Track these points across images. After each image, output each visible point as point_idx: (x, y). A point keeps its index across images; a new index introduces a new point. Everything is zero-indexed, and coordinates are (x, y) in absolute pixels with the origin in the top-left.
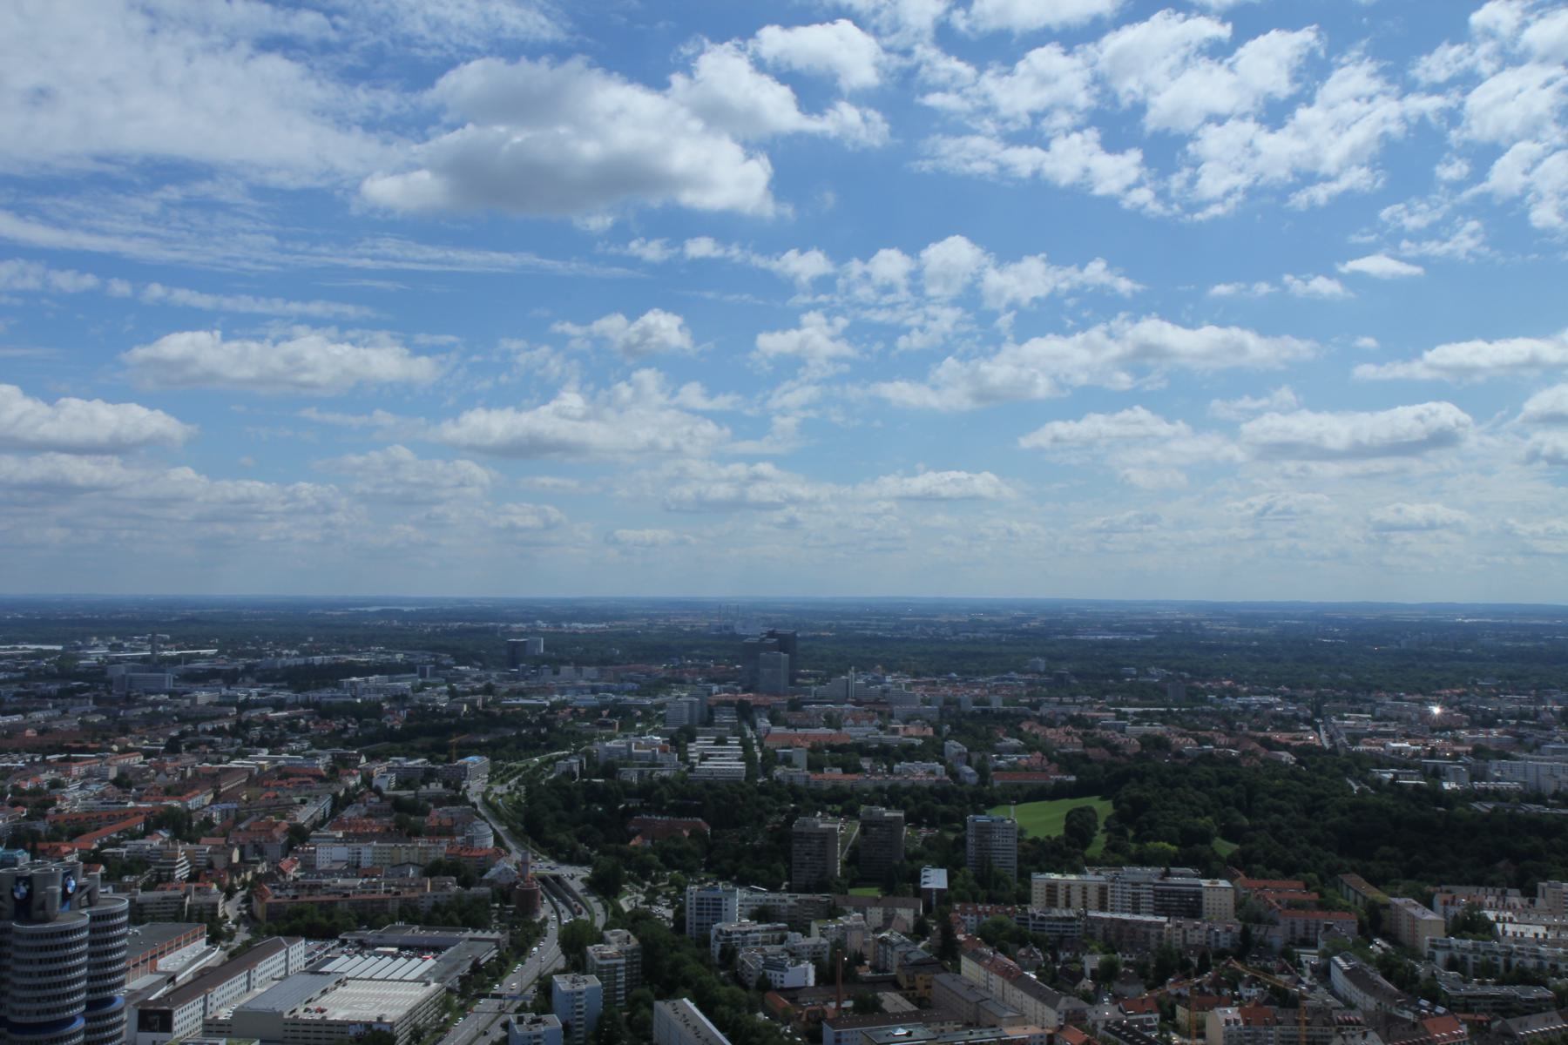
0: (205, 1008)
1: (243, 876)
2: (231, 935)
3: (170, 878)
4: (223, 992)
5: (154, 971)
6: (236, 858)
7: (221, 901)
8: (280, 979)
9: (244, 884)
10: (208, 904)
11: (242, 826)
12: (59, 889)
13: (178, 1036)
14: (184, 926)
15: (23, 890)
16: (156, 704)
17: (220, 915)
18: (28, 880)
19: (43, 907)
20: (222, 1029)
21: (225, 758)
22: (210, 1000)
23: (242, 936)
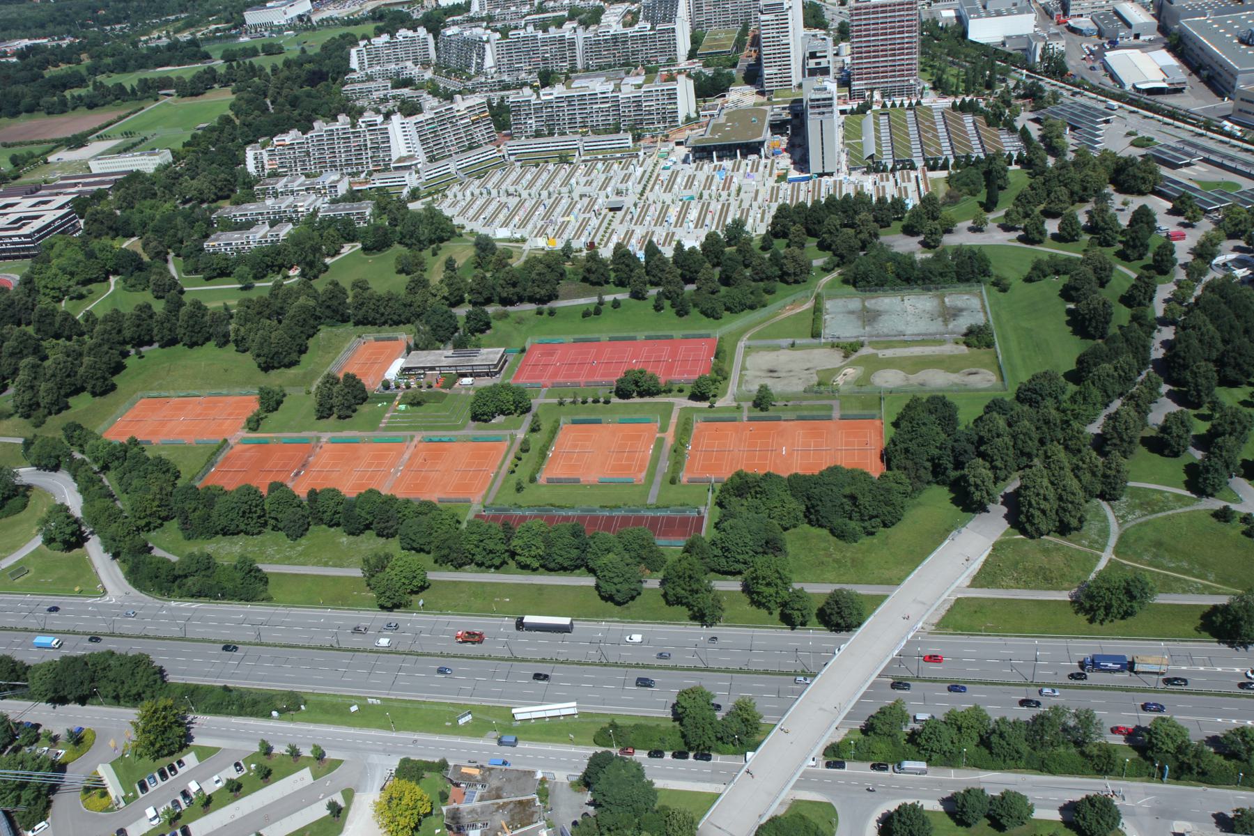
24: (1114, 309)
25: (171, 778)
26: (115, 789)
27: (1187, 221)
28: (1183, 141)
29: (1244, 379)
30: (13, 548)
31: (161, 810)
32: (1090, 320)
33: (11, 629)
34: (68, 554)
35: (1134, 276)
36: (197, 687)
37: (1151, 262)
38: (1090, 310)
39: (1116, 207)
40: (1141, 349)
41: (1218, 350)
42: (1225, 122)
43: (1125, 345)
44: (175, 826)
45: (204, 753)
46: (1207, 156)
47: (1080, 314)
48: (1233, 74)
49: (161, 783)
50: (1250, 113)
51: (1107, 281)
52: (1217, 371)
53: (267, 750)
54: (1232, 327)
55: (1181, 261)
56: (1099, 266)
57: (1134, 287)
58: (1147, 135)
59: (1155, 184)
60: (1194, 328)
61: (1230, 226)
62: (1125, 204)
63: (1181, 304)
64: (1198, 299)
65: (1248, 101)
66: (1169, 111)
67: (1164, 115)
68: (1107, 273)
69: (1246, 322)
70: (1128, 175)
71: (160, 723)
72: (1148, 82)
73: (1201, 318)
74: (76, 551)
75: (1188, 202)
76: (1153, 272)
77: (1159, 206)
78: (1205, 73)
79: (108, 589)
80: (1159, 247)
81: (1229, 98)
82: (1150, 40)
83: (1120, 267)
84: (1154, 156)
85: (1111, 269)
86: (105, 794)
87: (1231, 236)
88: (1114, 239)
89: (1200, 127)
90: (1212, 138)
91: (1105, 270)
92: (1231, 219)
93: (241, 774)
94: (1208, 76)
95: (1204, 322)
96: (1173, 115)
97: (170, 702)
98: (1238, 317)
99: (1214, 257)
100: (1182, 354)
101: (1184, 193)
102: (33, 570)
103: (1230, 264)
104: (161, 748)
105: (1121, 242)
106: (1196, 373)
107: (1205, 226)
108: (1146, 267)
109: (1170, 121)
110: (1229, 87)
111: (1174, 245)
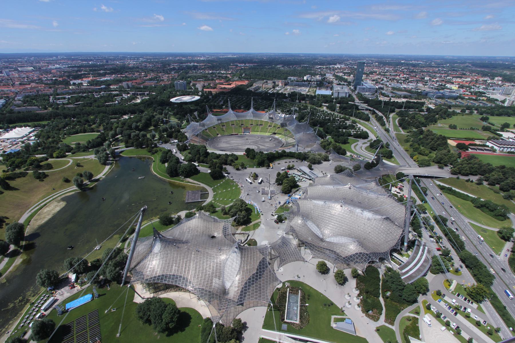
25: (466, 302)
26: (452, 287)
30: (489, 226)
31: (457, 304)
33: (469, 239)
34: (500, 239)
36: (497, 297)
44: (455, 310)
45: (479, 308)
49: (463, 300)
53: (497, 330)
71: (480, 292)
74: (503, 241)
79: (501, 255)
86: (450, 285)
93: (483, 324)
97: (488, 292)
102: (488, 234)
104: (472, 296)
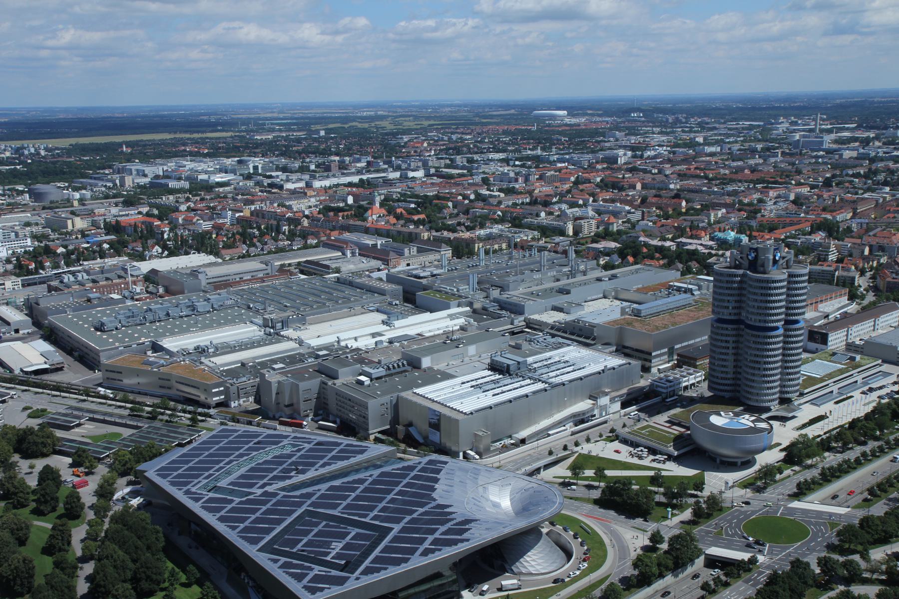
0: (847, 335)
1: (871, 263)
2: (863, 297)
3: (825, 260)
4: (858, 329)
5: (816, 310)
6: (867, 252)
7: (857, 277)
8: (895, 327)
9: (872, 268)
10: (849, 277)
11: (871, 233)
12: (771, 257)
13: (832, 348)
14: (834, 288)
15: (753, 255)
16: (817, 157)
17: (856, 284)
18: (756, 250)
19: (763, 266)
20: (857, 349)
21: (860, 192)
22: (850, 332)
23: (870, 297)
24: (36, 563)
27: (86, 470)
28: (71, 408)
29: (156, 587)
32: (14, 579)
35: (50, 526)
37: (63, 511)
38: (12, 571)
39: (24, 472)
40: (66, 591)
41: (131, 570)
42: (100, 389)
43: (50, 592)
46: (91, 416)
47: (4, 577)
48: (97, 353)
50: (115, 380)
51: (26, 539)
52: (133, 588)
54: (137, 548)
55: (88, 504)
56: (15, 527)
57: (52, 537)
58: (40, 407)
59: (54, 445)
60: (107, 557)
61: (120, 467)
62: (32, 467)
63: (95, 540)
64: (106, 532)
65: (111, 371)
66: (54, 386)
67: (51, 390)
68: (24, 532)
69: (147, 540)
70: (29, 443)
72: (32, 365)
73: (112, 547)
75: (84, 455)
76: (64, 520)
77: (61, 463)
78: (76, 354)
80: (67, 497)
81: (99, 370)
82: (28, 333)
83: (36, 523)
84: (49, 423)
85: (28, 527)
87: (123, 474)
88: (26, 499)
89: (81, 395)
90: (93, 402)
91: (22, 529)
92: (119, 461)
94: (79, 355)
95: (114, 550)
96: (58, 388)
98: (139, 538)
99: (113, 495)
100: (102, 583)
101: (79, 448)
103: (127, 497)
105: (33, 501)
106: (116, 596)
107: (102, 470)
108: (59, 517)
109: (58, 393)
110: (97, 363)
111: (78, 493)
